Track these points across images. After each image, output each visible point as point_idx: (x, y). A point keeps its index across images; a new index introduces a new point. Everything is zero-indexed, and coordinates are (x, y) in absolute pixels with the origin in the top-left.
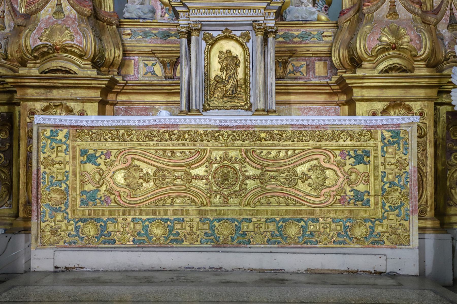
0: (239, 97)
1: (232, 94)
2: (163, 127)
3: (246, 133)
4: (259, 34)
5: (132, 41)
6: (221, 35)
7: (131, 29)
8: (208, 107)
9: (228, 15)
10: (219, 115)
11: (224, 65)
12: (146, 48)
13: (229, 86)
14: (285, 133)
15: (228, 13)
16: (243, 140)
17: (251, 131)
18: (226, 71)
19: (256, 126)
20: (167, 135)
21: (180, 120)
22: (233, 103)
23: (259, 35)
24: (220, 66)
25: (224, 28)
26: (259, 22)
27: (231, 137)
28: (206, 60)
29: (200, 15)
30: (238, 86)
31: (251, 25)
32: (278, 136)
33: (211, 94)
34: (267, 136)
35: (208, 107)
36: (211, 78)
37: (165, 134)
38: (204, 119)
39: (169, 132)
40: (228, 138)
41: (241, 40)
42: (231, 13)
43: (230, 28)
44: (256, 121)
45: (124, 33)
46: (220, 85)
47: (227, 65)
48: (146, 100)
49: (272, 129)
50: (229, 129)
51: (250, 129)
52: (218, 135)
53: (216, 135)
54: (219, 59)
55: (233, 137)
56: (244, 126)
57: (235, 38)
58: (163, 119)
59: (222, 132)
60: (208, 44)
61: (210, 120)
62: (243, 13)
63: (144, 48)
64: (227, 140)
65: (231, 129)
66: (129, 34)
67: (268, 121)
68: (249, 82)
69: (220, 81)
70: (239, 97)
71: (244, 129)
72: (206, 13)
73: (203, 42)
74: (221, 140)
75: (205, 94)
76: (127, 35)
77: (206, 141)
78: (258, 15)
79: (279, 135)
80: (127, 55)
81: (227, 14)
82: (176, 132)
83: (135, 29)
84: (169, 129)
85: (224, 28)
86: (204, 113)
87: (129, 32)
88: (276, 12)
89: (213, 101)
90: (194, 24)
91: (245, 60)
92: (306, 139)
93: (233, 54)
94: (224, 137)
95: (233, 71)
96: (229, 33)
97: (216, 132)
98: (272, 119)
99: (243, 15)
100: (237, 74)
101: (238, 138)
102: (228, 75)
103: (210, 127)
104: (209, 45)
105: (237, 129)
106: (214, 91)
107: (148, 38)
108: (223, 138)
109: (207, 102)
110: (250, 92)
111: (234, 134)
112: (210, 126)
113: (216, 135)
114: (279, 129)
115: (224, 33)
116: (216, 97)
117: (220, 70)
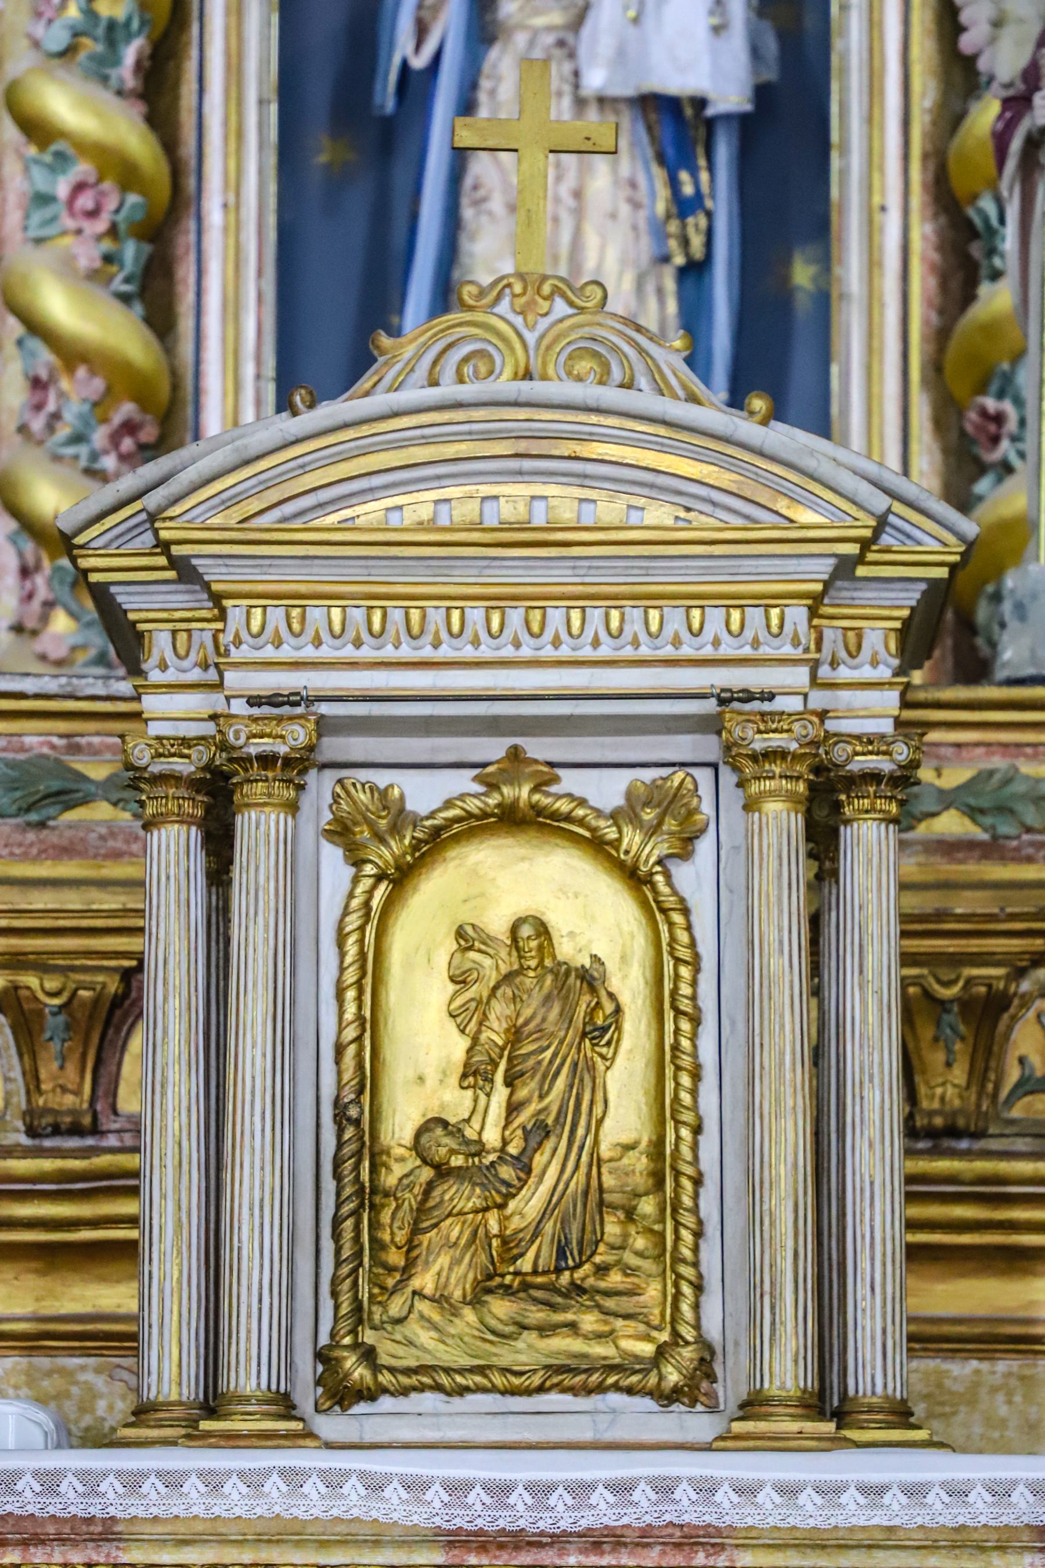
0: (608, 1294)
1: (558, 1271)
4: (772, 794)
6: (473, 805)
8: (360, 1373)
9: (526, 652)
11: (495, 1035)
15: (525, 637)
18: (509, 1082)
21: (133, 1481)
22: (563, 1344)
24: (464, 1043)
26: (766, 706)
28: (351, 994)
29: (309, 652)
30: (601, 1203)
31: (712, 725)
33: (391, 1269)
35: (360, 1373)
36: (386, 1138)
38: (323, 1473)
42: (548, 635)
44: (747, 1490)
47: (516, 1035)
54: (451, 988)
57: (581, 822)
60: (369, 869)
61: (375, 1485)
62: (643, 637)
67: (844, 1498)
68: (689, 1170)
69: (457, 1161)
70: (608, 1294)
72: (351, 634)
73: (332, 855)
75: (338, 1264)
78: (765, 651)
81: (517, 644)
86: (329, 1426)
88: (907, 622)
89: (399, 1321)
90: (255, 720)
95: (561, 1083)
96: (536, 789)
98: (875, 1478)
99: (645, 651)
100: (598, 1110)
102: (524, 1117)
104: (379, 878)
106: (411, 1245)
109: (354, 1332)
115: (492, 786)
116: (429, 1290)
117: (464, 1076)
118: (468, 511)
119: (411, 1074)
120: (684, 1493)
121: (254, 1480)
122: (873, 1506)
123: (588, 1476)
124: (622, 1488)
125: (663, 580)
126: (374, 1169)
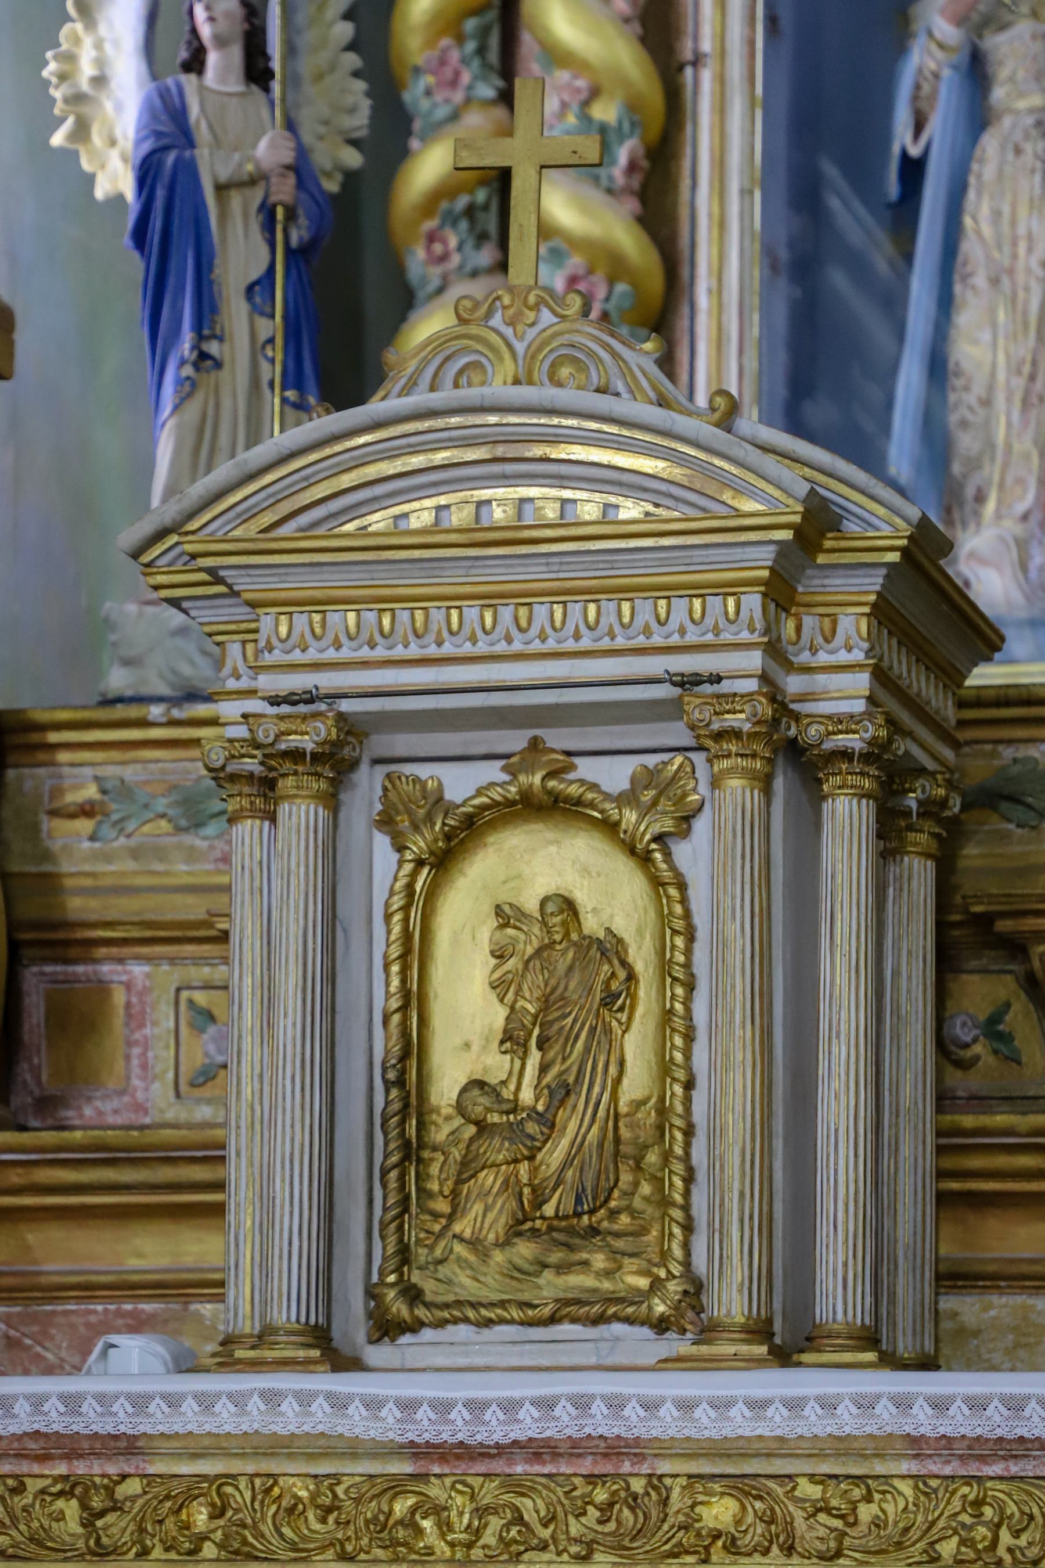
0: (617, 1235)
1: (578, 1215)
2: (43, 1458)
3: (601, 1496)
4: (730, 771)
5: (108, 857)
6: (496, 794)
7: (100, 771)
8: (399, 1308)
9: (517, 646)
10: (480, 1361)
12: (190, 899)
13: (554, 1155)
14: (868, 1499)
15: (514, 632)
16: (574, 1549)
17: (638, 1485)
18: (540, 1047)
19: (664, 1448)
20: (71, 1508)
23: (735, 783)
24: (502, 1013)
25: (516, 740)
26: (715, 688)
27: (495, 1523)
28: (395, 968)
29: (331, 654)
30: (617, 1153)
32: (822, 1517)
33: (436, 1215)
34: (750, 1518)
35: (399, 1308)
36: (434, 1099)
37: (60, 1504)
38: (298, 1395)
39: (86, 1491)
40: (478, 1533)
41: (630, 817)
42: (534, 631)
43: (558, 739)
44: (650, 1406)
45: (56, 805)
46: (498, 1150)
47: (546, 1003)
48: (134, 1263)
49: (780, 1467)
50: (481, 1467)
51: (626, 1467)
52: (413, 1511)
53: (400, 1507)
54: (493, 961)
55: (507, 1526)
56: (576, 1448)
57: (592, 805)
58: (27, 1397)
59: (435, 1491)
60: (409, 856)
62: (617, 629)
63: (179, 899)
64: (470, 1546)
65: (499, 1466)
66: (86, 810)
67: (733, 1412)
68: (678, 1122)
69: (494, 1118)
70: (617, 1235)
71: (586, 1466)
72: (365, 636)
73: (382, 842)
74: (430, 1551)
75: (385, 1210)
76: (73, 816)
77: (330, 1554)
78: (726, 637)
79: (828, 1510)
80: (73, 952)
81: (509, 640)
82: (133, 1487)
83: (130, 773)
84: (81, 1468)
85: (516, 740)
87: (91, 792)
88: (875, 606)
89: (441, 1262)
90: (282, 718)
91: (664, 967)
92: (1023, 1541)
93: (591, 925)
94: (451, 1529)
95: (580, 1045)
96: (551, 775)
97: (396, 1486)
98: (760, 1393)
99: (620, 642)
100: (613, 1070)
101: (546, 1533)
102: (548, 1078)
103: (354, 1456)
104: (420, 863)
105: (537, 1469)
106: (455, 1193)
107: (210, 830)
108: (445, 1527)
109: (398, 1270)
110: (687, 1194)
111: (518, 1501)
112: (354, 1449)
113: (400, 1507)
114: (825, 1468)
115: (512, 772)
116: (467, 1234)
117: (502, 1042)
118: (459, 517)
119: (458, 1041)
120: (598, 1408)
121: (238, 1399)
122: (758, 1418)
123: (517, 1394)
124: (546, 1404)
125: (627, 574)
126: (421, 1126)
